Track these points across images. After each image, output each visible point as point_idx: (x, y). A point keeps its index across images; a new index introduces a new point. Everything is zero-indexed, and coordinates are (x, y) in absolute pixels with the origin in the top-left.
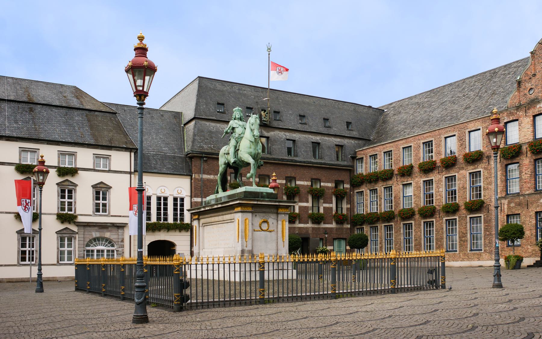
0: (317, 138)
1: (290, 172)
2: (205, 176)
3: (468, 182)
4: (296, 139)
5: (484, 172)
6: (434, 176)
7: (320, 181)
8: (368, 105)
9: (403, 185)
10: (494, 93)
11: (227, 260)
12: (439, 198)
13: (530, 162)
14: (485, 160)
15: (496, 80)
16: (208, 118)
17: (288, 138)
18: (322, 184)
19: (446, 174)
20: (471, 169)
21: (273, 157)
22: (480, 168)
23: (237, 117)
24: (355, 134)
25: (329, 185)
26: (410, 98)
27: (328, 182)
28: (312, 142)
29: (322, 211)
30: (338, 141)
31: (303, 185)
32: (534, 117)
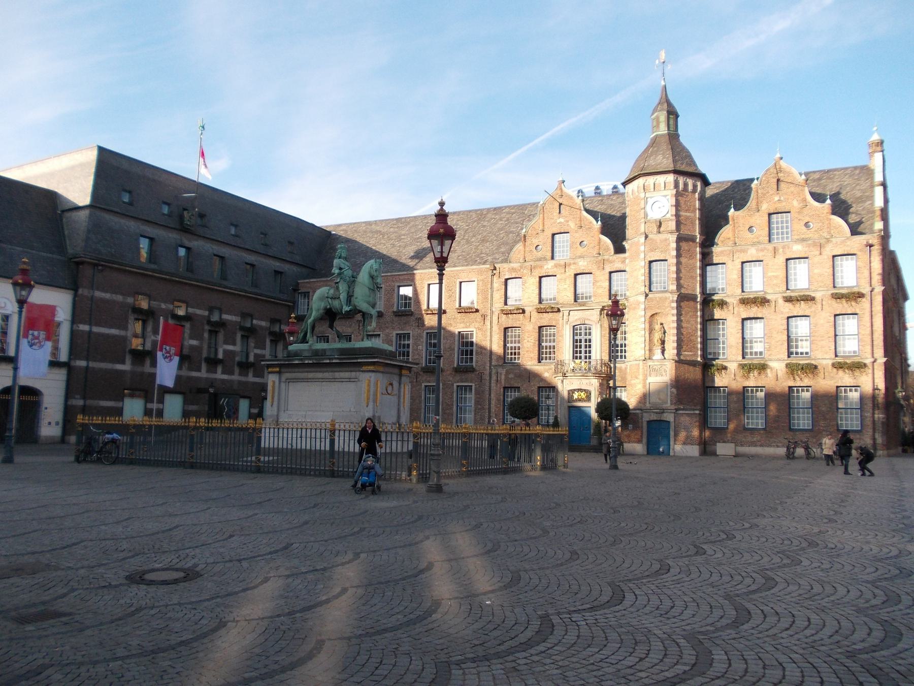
2: (98, 294)
4: (227, 255)
7: (252, 316)
10: (484, 241)
11: (309, 426)
15: (485, 224)
16: (108, 208)
17: (215, 253)
18: (255, 322)
23: (343, 255)
24: (297, 259)
25: (263, 324)
26: (369, 223)
27: (262, 320)
30: (277, 265)
31: (231, 321)
32: (540, 278)
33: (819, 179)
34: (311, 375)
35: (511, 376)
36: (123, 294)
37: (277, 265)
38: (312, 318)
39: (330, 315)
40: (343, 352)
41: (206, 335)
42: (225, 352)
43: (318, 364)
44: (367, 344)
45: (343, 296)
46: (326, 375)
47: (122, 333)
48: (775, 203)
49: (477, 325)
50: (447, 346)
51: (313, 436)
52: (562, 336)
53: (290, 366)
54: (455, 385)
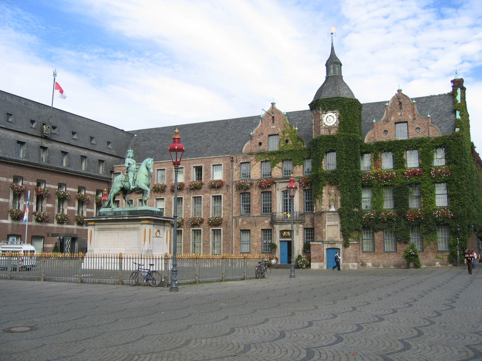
0: (22, 138)
1: (62, 179)
3: (211, 203)
5: (223, 197)
6: (183, 195)
7: (85, 189)
8: (121, 129)
9: (156, 199)
12: (187, 212)
13: (258, 193)
14: (224, 187)
19: (193, 195)
20: (215, 193)
21: (51, 165)
22: (221, 193)
24: (113, 152)
27: (91, 191)
28: (81, 156)
29: (66, 212)
30: (100, 156)
33: (426, 102)
34: (112, 226)
35: (245, 223)
36: (6, 177)
37: (100, 156)
38: (113, 193)
39: (124, 191)
40: (131, 213)
41: (57, 201)
42: (68, 210)
43: (117, 219)
44: (145, 208)
45: (131, 180)
46: (121, 226)
47: (7, 200)
48: (398, 116)
49: (224, 192)
50: (205, 205)
51: (116, 262)
52: (276, 198)
53: (100, 220)
54: (211, 229)
